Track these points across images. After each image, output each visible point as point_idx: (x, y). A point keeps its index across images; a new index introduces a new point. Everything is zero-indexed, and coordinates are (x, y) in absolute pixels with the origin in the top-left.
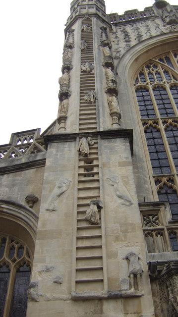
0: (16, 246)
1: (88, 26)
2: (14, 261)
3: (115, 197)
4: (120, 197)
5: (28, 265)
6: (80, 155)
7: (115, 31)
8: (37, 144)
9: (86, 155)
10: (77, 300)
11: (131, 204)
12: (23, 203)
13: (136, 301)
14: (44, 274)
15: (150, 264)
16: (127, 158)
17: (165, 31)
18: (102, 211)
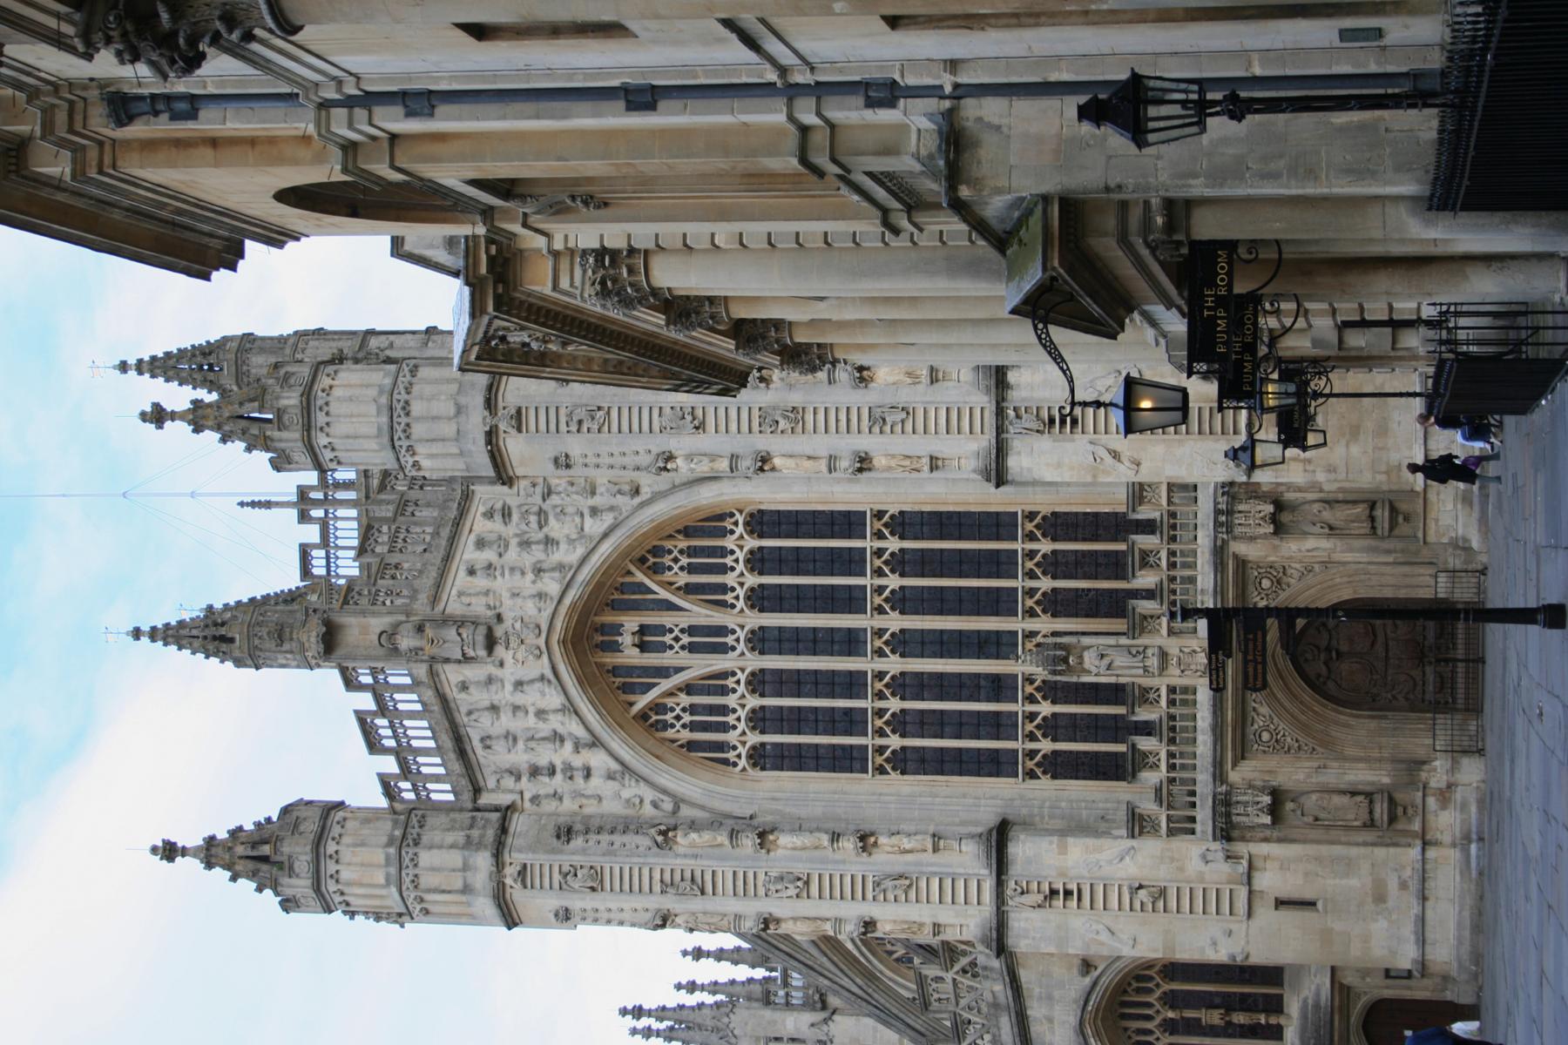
0: (1135, 985)
1: (576, 875)
2: (1158, 985)
3: (1120, 865)
4: (1121, 859)
5: (1165, 966)
6: (1039, 906)
7: (517, 797)
8: (957, 967)
9: (1045, 898)
10: (1250, 915)
11: (1133, 848)
12: (1088, 980)
13: (1254, 859)
14: (1218, 948)
15: (1215, 839)
16: (1051, 843)
17: (544, 666)
18: (1144, 883)
